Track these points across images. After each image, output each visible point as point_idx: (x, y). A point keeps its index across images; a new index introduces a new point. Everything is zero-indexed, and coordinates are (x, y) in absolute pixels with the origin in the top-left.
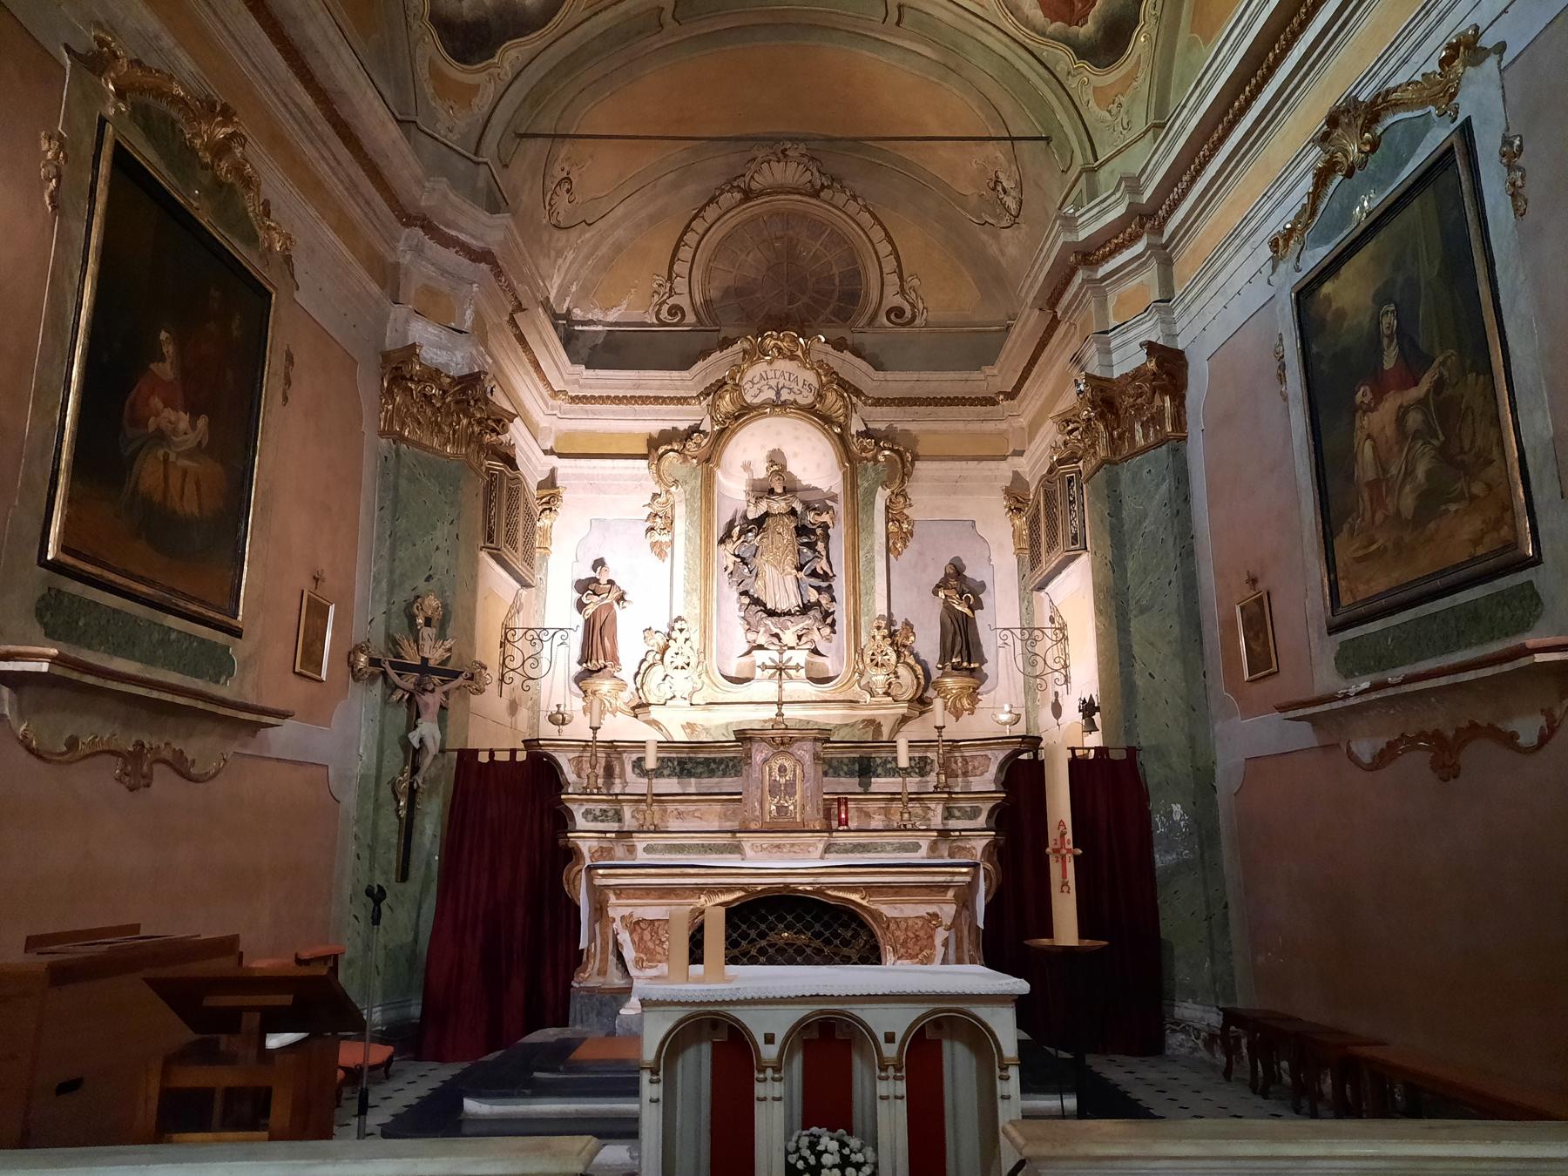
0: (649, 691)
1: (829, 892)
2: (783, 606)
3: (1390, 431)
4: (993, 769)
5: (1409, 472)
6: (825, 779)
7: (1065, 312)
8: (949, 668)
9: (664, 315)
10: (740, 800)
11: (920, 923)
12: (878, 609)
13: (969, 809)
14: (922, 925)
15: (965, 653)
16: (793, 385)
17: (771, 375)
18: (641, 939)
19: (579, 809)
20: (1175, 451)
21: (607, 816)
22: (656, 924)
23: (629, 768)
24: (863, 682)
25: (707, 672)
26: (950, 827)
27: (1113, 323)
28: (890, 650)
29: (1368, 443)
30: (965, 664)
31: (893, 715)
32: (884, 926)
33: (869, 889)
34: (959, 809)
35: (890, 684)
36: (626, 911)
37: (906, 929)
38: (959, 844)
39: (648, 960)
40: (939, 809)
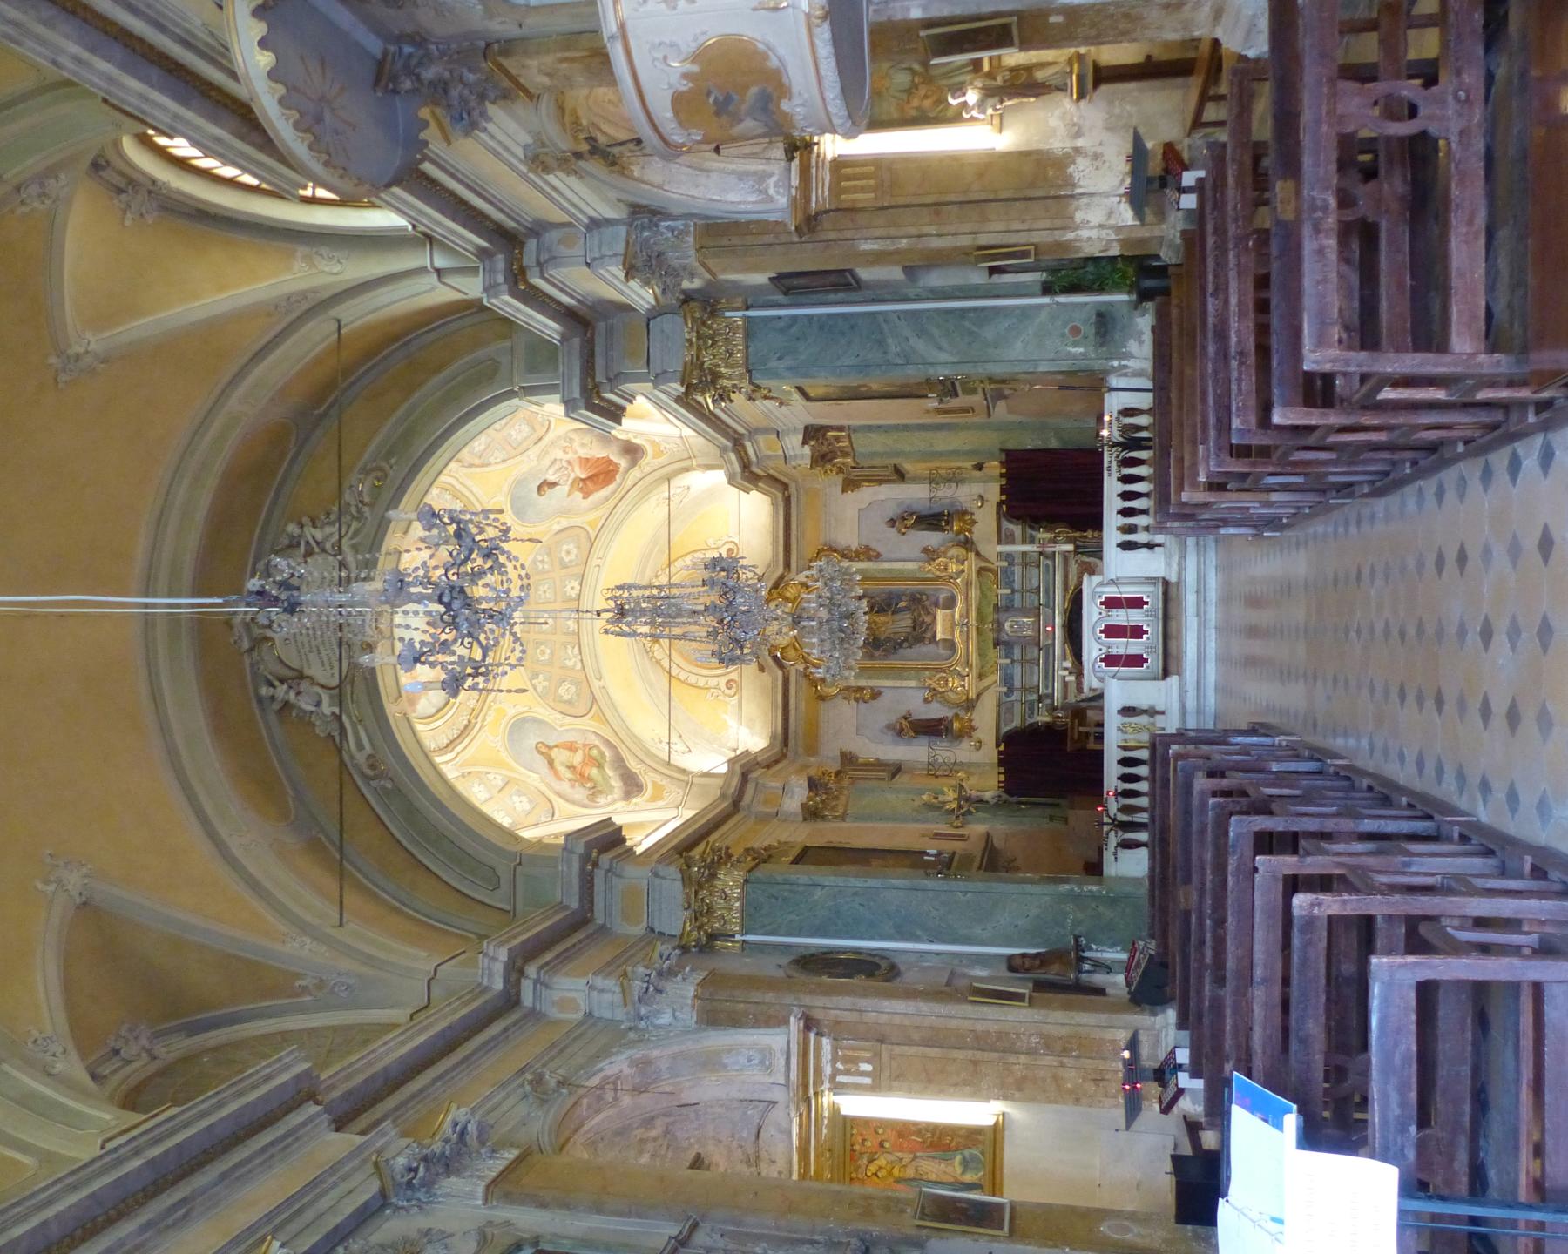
2: (909, 622)
4: (1011, 526)
9: (731, 692)
20: (855, 431)
27: (780, 452)
33: (1066, 589)
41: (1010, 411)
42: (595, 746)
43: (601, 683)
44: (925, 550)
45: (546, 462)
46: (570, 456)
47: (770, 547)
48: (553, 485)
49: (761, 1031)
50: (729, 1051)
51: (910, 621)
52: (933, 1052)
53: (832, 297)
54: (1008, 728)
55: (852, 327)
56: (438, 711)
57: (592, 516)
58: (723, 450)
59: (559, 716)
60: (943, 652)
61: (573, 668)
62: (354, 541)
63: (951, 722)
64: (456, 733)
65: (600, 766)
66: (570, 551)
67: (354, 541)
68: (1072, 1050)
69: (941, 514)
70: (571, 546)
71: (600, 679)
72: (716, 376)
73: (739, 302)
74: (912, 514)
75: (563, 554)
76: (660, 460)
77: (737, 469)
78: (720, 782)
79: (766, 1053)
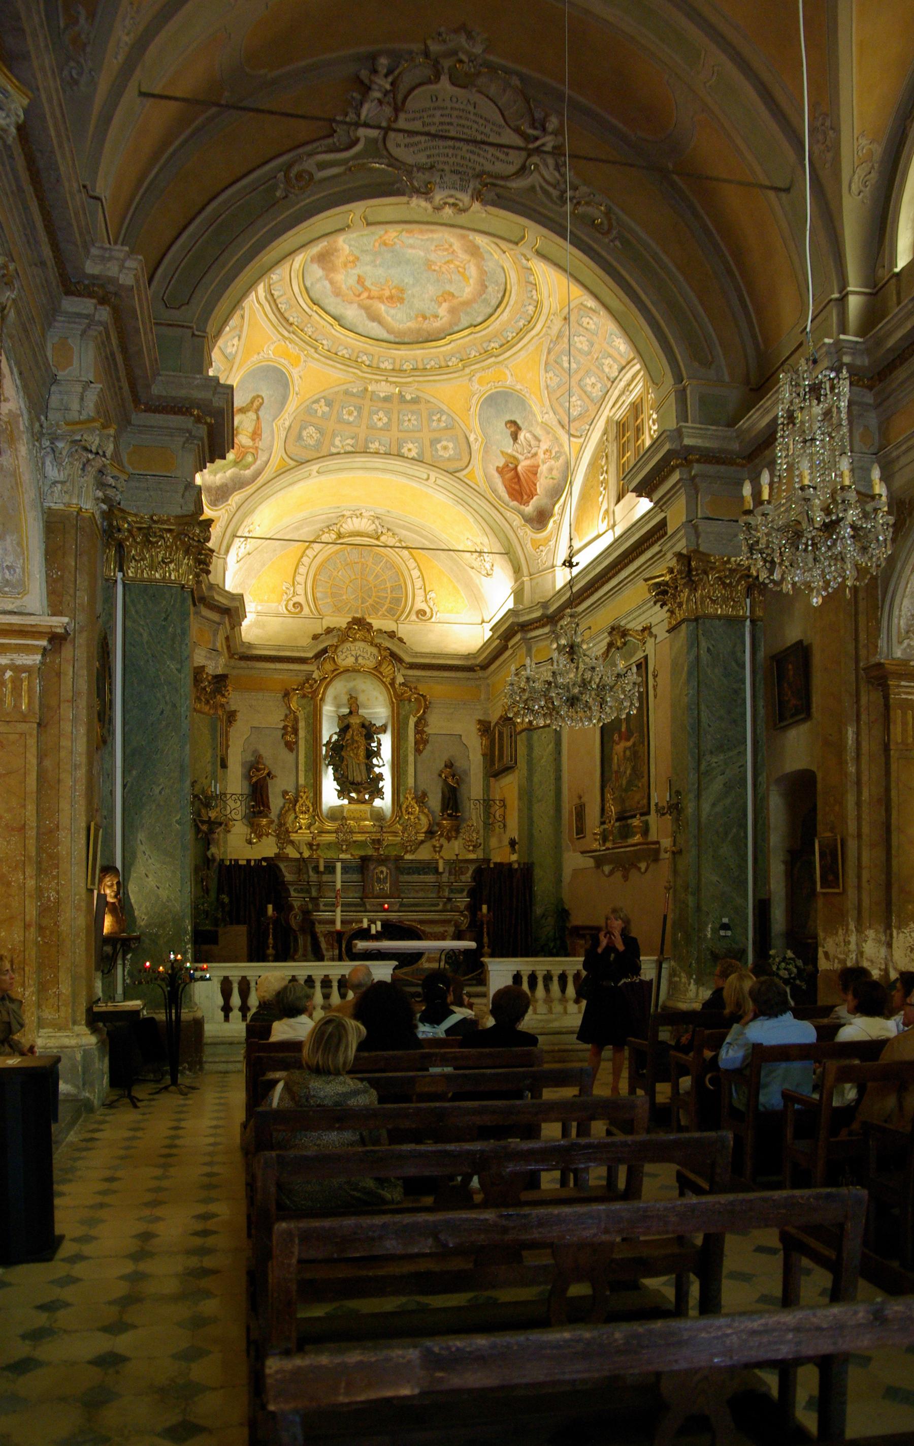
2: (358, 779)
3: (622, 754)
4: (470, 872)
5: (625, 772)
7: (512, 647)
8: (445, 816)
9: (290, 607)
16: (365, 655)
17: (353, 648)
29: (616, 757)
41: (576, 872)
42: (255, 460)
43: (314, 473)
44: (425, 795)
45: (539, 432)
46: (541, 455)
47: (427, 650)
48: (515, 437)
49: (44, 585)
50: (19, 544)
51: (359, 780)
52: (32, 781)
53: (761, 703)
55: (735, 721)
56: (306, 289)
57: (479, 474)
58: (545, 605)
59: (287, 424)
61: (333, 445)
62: (538, 189)
63: (266, 816)
64: (283, 307)
65: (236, 463)
66: (447, 449)
67: (538, 189)
68: (44, 937)
70: (452, 452)
71: (318, 472)
72: (693, 585)
73: (759, 613)
75: (444, 443)
76: (529, 545)
77: (522, 619)
78: (221, 586)
79: (20, 588)
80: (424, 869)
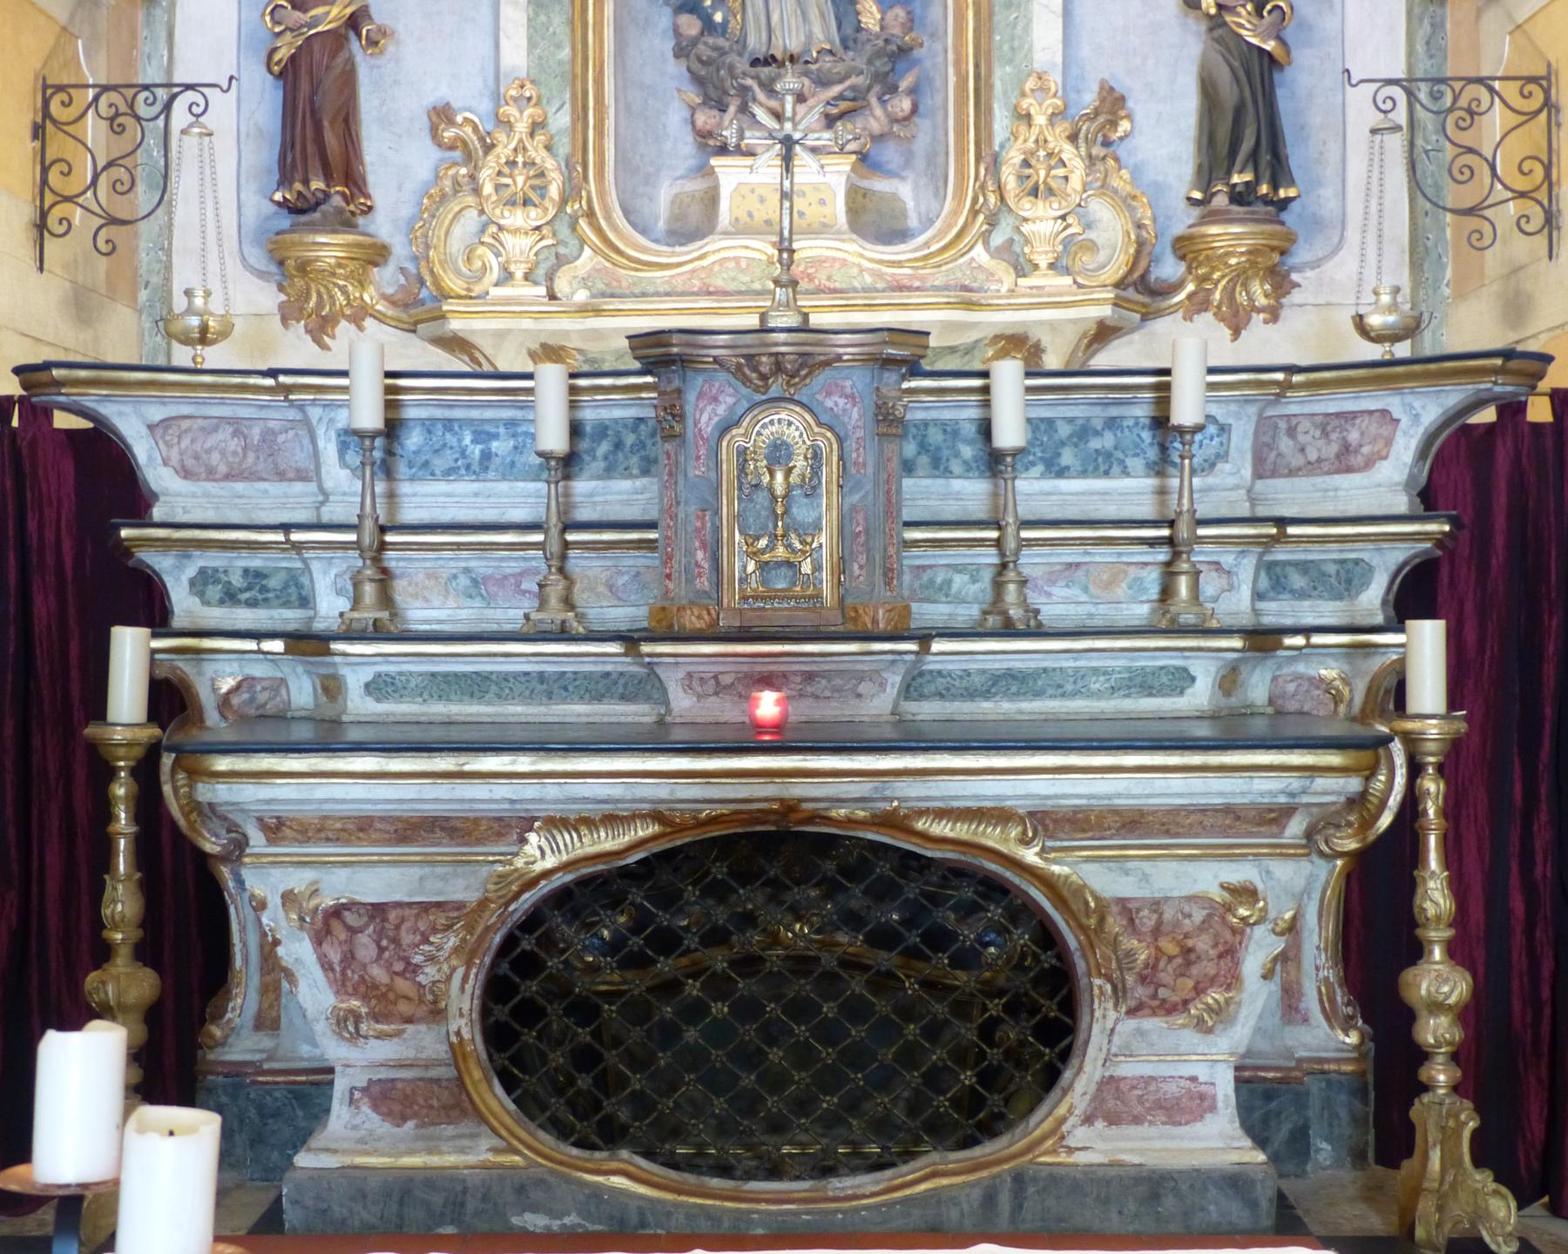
0: (443, 263)
1: (920, 825)
6: (907, 483)
8: (1221, 201)
10: (649, 545)
11: (1199, 915)
12: (1037, 45)
13: (1332, 569)
14: (1208, 919)
15: (1265, 157)
18: (349, 957)
19: (180, 568)
21: (264, 589)
22: (393, 915)
23: (329, 448)
24: (998, 239)
25: (590, 214)
26: (1268, 621)
28: (1068, 152)
30: (1264, 189)
31: (1073, 321)
32: (1093, 922)
34: (1304, 567)
35: (1067, 242)
36: (298, 880)
37: (1157, 931)
38: (1301, 668)
39: (376, 1017)
40: (1247, 570)
44: (1113, 104)
51: (794, 45)
54: (142, 450)
60: (664, 197)
69: (1279, 171)
74: (1279, 39)
80: (1084, 432)
